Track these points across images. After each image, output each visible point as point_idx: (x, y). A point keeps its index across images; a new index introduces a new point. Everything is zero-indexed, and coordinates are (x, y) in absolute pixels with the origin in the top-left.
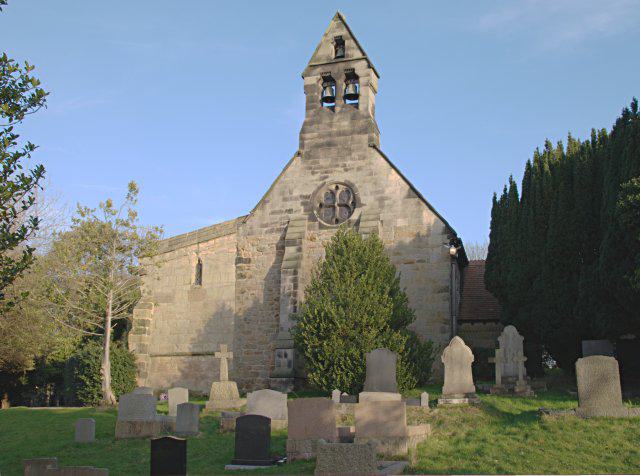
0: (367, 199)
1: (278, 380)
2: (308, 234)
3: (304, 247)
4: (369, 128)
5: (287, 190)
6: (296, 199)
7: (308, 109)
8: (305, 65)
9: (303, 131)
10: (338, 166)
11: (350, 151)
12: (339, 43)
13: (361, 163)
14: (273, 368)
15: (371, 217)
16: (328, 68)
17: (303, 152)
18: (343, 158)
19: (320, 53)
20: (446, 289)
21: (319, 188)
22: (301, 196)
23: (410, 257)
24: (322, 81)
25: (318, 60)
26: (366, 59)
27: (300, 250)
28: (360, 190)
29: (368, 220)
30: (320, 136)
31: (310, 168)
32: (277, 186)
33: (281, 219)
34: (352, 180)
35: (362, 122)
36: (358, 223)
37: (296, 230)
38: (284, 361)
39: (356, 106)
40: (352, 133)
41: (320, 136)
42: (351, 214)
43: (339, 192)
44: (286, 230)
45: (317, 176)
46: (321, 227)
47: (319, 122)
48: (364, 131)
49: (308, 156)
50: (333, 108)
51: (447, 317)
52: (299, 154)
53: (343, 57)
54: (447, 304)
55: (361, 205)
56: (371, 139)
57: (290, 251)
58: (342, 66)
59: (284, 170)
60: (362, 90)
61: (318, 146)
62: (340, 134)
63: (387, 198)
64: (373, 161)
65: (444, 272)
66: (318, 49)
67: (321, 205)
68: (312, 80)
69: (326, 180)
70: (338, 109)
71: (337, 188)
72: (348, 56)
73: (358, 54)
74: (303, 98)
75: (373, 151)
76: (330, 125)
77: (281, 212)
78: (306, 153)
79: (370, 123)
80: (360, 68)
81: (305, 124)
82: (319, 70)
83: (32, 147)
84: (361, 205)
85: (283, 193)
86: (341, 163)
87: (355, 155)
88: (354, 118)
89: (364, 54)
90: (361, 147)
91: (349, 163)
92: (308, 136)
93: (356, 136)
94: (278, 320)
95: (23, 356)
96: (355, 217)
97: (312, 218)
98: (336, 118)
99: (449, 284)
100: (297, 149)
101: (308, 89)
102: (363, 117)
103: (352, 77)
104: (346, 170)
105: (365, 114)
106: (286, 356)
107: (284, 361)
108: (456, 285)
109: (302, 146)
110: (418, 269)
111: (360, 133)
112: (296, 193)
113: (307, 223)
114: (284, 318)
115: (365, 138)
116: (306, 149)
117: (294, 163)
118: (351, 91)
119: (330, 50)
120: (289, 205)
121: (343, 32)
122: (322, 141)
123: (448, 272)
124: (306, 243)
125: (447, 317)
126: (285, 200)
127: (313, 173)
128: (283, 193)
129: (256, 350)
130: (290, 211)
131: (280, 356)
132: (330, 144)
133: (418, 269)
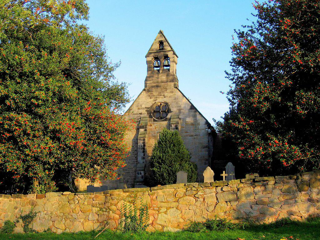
0: (174, 109)
1: (138, 183)
2: (149, 124)
3: (147, 129)
4: (174, 80)
5: (139, 105)
6: (144, 109)
7: (148, 71)
8: (147, 52)
9: (146, 80)
10: (161, 95)
11: (166, 89)
12: (161, 43)
13: (171, 94)
14: (135, 179)
15: (176, 117)
16: (157, 54)
17: (146, 89)
18: (163, 92)
19: (153, 47)
20: (206, 147)
21: (153, 105)
22: (146, 108)
23: (192, 134)
24: (154, 59)
25: (153, 50)
26: (173, 51)
27: (146, 130)
28: (170, 106)
29: (174, 118)
30: (153, 83)
31: (150, 96)
32: (135, 103)
33: (137, 117)
34: (167, 102)
35: (171, 78)
36: (170, 119)
37: (144, 122)
38: (140, 176)
39: (169, 70)
40: (167, 82)
41: (153, 83)
42: (167, 115)
43: (162, 106)
44: (140, 122)
45: (152, 99)
46: (154, 120)
47: (153, 77)
48: (172, 81)
49: (148, 91)
50: (159, 71)
51: (207, 158)
52: (144, 90)
53: (163, 49)
54: (207, 153)
55: (171, 112)
56: (175, 85)
57: (142, 130)
58: (162, 53)
59: (138, 96)
60: (171, 64)
61: (153, 87)
62: (162, 82)
63: (182, 109)
64: (176, 94)
65: (205, 140)
66: (152, 46)
67: (154, 111)
68: (150, 59)
69: (156, 101)
70: (161, 71)
71: (161, 104)
72: (165, 49)
73: (169, 49)
74: (146, 66)
75: (176, 89)
76: (158, 78)
77: (137, 114)
78: (147, 90)
79: (174, 78)
80: (170, 54)
81: (147, 77)
82: (153, 54)
83: (225, 77)
84: (171, 112)
85: (138, 106)
86: (162, 94)
87: (168, 91)
88: (168, 75)
89: (172, 49)
90: (171, 88)
91: (166, 94)
92: (148, 82)
93: (169, 83)
94: (137, 159)
95: (112, 124)
96: (169, 116)
97: (151, 117)
98: (160, 75)
99: (208, 144)
100: (144, 88)
101: (148, 62)
102: (172, 75)
103: (166, 57)
104: (165, 97)
105: (172, 74)
106: (141, 174)
107: (140, 176)
108: (211, 144)
109: (146, 86)
110: (195, 139)
111: (170, 82)
112: (143, 106)
113: (148, 119)
114: (140, 159)
115: (172, 84)
116: (147, 88)
117: (142, 93)
118: (166, 63)
119: (157, 46)
120: (140, 111)
121: (163, 39)
122: (154, 85)
123: (207, 140)
124: (148, 127)
125: (207, 158)
126: (139, 109)
127: (151, 98)
128: (138, 106)
129: (127, 172)
130: (141, 114)
131: (138, 174)
132: (157, 86)
133: (195, 139)
